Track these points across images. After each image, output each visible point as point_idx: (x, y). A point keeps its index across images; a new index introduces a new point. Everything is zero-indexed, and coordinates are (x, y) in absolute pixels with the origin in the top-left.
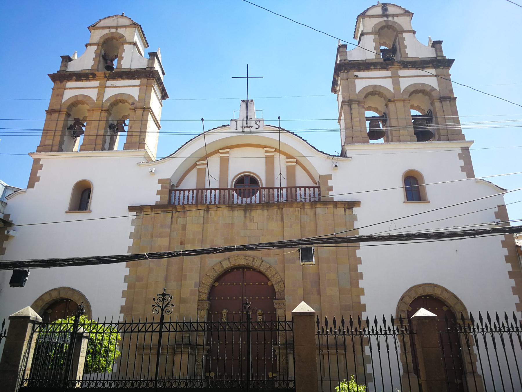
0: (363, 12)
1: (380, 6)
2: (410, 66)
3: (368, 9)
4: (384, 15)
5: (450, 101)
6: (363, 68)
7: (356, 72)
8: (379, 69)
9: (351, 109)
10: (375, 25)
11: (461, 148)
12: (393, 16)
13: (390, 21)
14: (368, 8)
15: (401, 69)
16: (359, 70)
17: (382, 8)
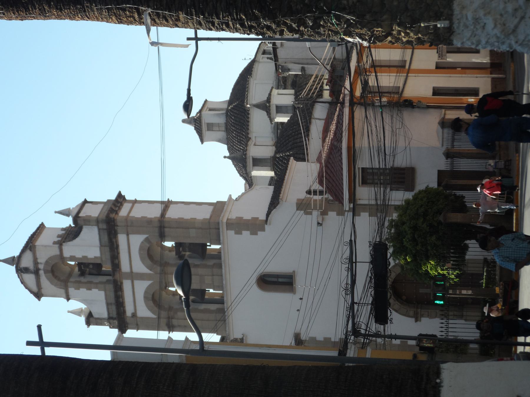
0: (32, 295)
1: (21, 275)
2: (117, 262)
3: (26, 288)
4: (36, 272)
5: (164, 227)
6: (122, 309)
7: (126, 315)
8: (121, 292)
9: (179, 326)
10: (52, 283)
11: (227, 230)
12: (36, 263)
13: (44, 267)
14: (26, 288)
15: (120, 269)
16: (124, 312)
17: (24, 273)
